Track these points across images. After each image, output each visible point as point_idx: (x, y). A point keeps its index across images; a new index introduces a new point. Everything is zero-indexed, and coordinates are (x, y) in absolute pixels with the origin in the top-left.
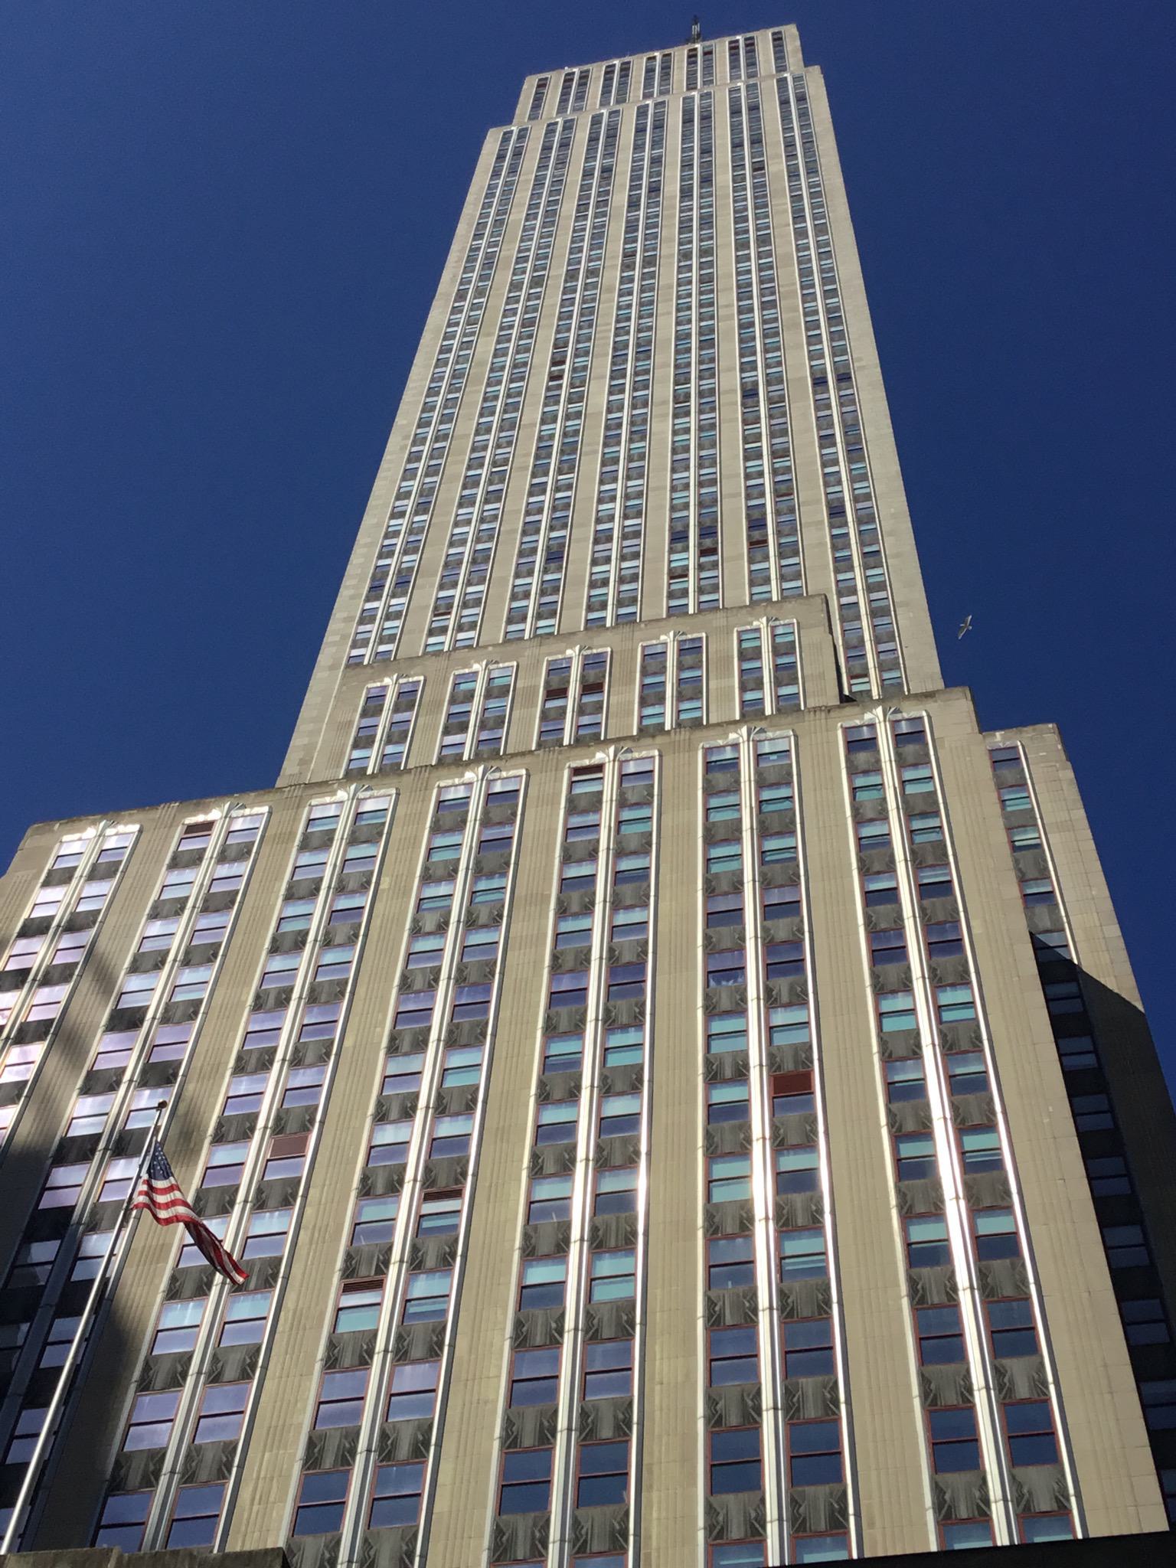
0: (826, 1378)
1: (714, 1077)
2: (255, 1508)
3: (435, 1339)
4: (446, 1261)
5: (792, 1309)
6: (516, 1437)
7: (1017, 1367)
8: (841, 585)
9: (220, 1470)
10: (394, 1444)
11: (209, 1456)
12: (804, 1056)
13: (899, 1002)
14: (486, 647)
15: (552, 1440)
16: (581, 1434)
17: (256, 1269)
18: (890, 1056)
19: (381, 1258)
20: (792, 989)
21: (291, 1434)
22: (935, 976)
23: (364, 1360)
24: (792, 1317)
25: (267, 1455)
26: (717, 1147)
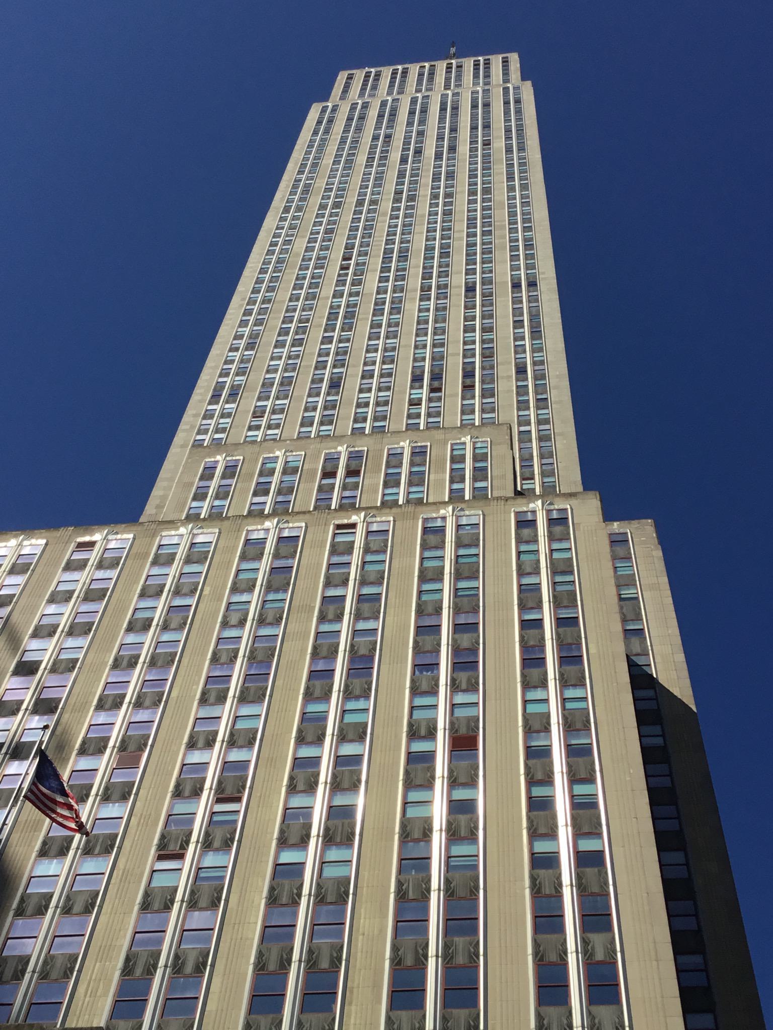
0: (472, 938)
1: (413, 734)
2: (87, 999)
3: (216, 895)
4: (227, 844)
5: (453, 891)
6: (264, 964)
7: (597, 939)
8: (516, 335)
9: (65, 972)
10: (183, 963)
11: (59, 963)
12: (473, 724)
13: (538, 694)
14: (285, 441)
15: (288, 968)
16: (317, 898)
17: (100, 840)
18: (530, 729)
19: (185, 839)
20: (469, 680)
21: (115, 953)
22: (563, 678)
23: (167, 906)
24: (453, 896)
25: (98, 964)
26: (412, 781)
